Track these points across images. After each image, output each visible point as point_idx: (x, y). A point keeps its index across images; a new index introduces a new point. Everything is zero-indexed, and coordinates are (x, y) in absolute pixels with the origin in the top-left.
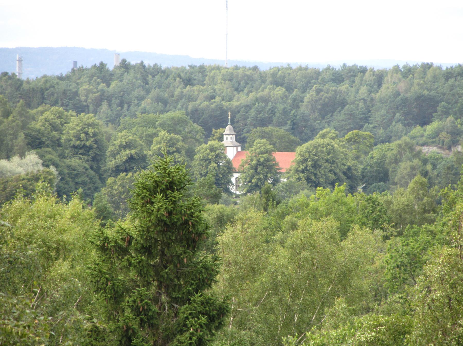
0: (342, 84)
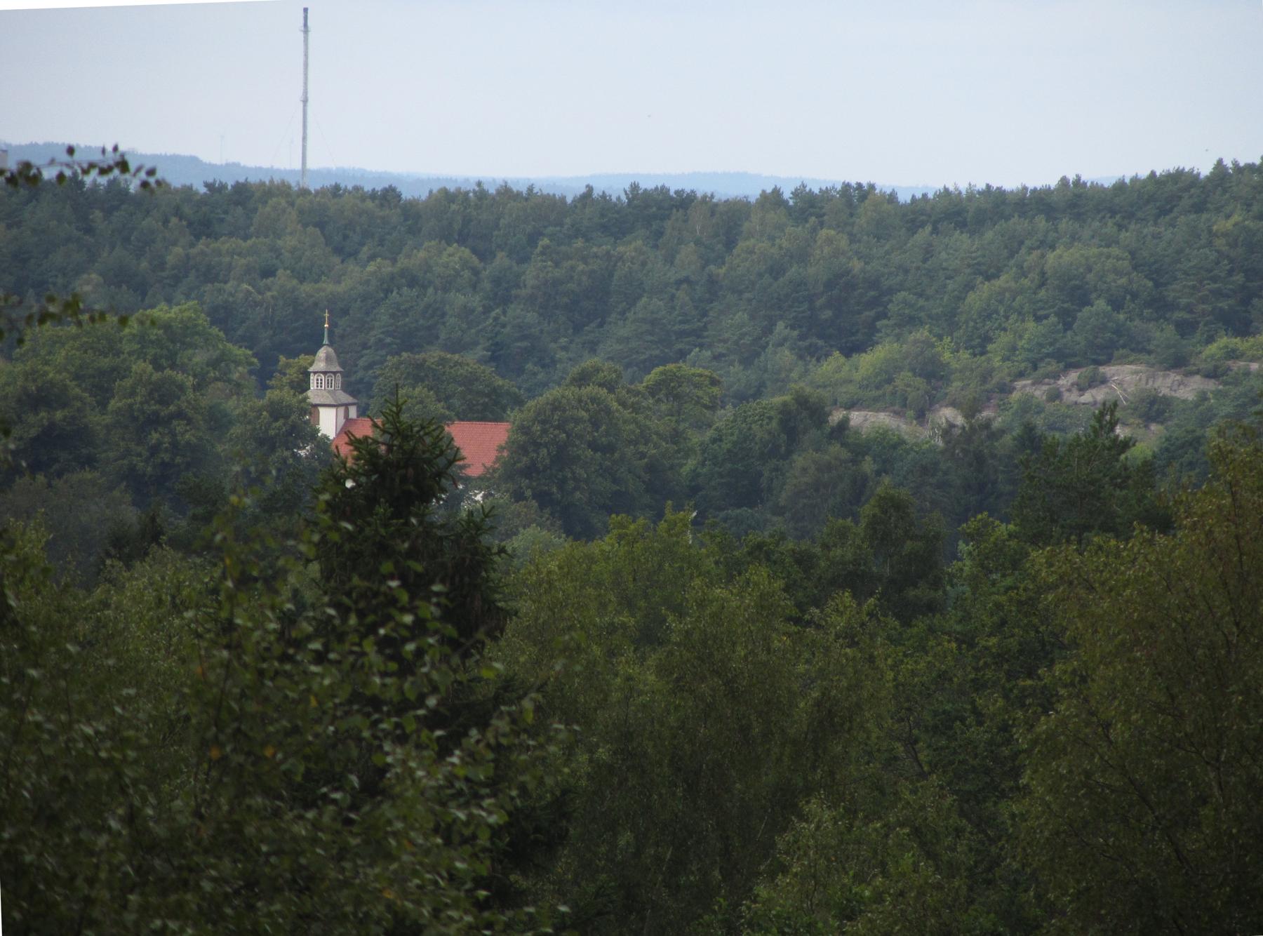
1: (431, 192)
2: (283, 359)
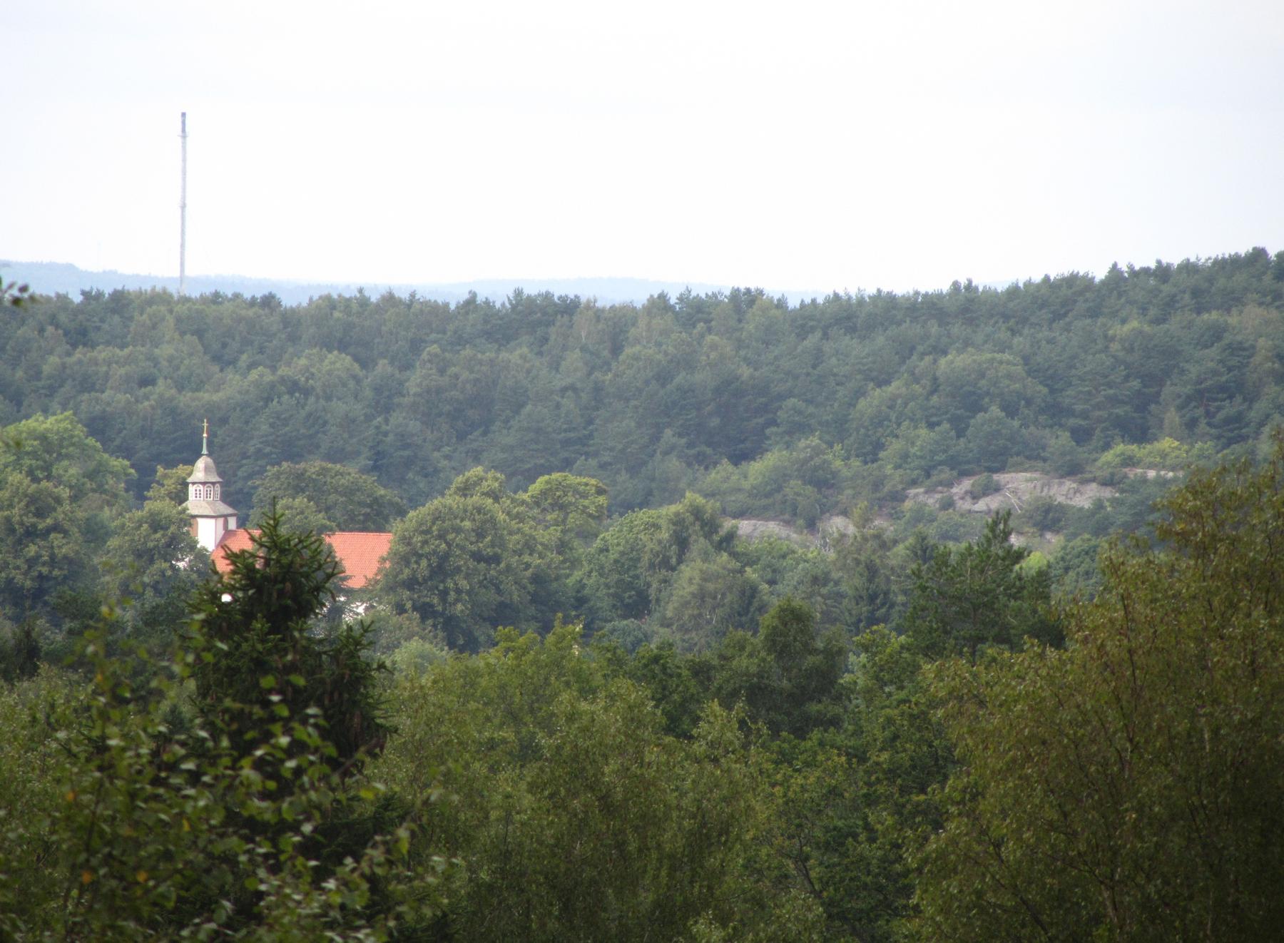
0: (513, 344)
1: (311, 299)
2: (160, 470)
